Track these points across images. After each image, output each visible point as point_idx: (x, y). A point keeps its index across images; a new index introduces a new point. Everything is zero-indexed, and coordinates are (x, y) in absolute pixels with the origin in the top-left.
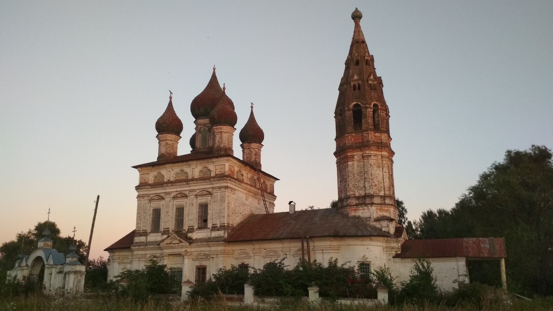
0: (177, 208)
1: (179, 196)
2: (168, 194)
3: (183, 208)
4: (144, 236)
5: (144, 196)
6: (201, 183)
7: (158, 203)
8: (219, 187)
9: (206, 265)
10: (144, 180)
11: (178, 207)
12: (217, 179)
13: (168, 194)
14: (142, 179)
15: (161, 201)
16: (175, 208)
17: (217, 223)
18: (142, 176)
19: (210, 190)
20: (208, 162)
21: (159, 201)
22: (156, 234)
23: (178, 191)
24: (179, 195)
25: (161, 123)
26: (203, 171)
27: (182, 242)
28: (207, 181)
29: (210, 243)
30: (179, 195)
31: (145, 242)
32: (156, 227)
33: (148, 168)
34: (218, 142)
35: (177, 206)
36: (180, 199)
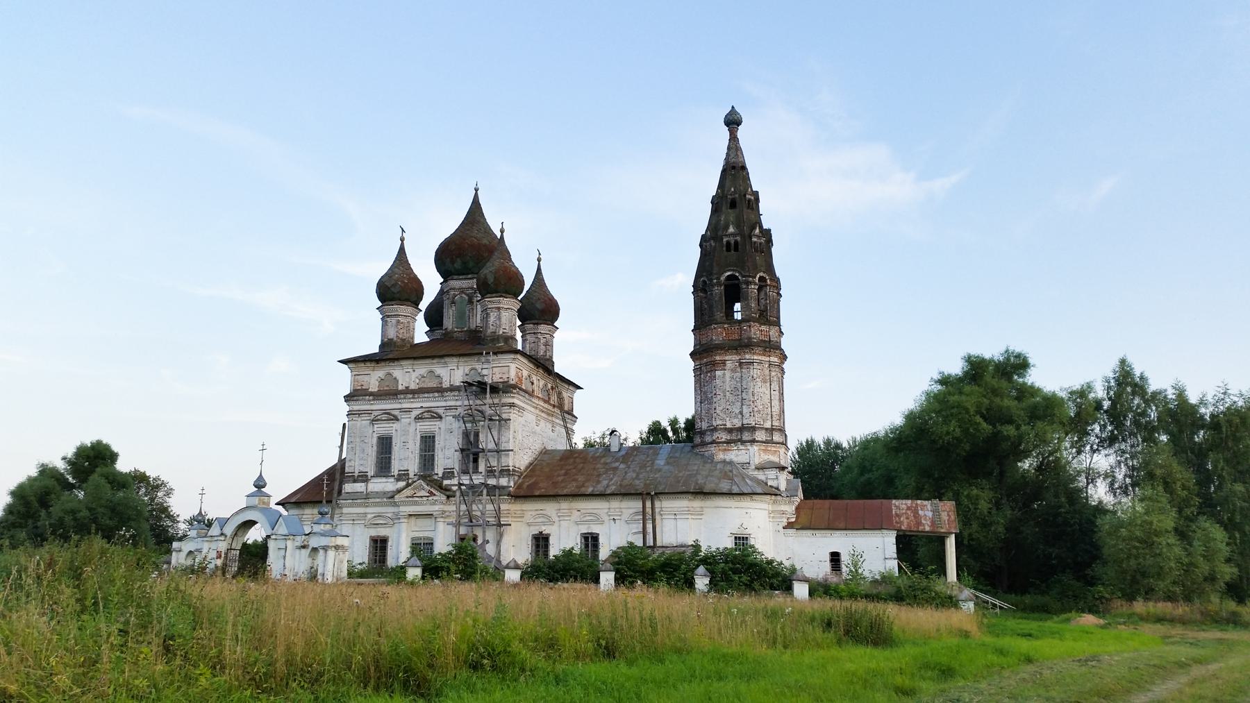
2: (405, 412)
3: (434, 437)
4: (363, 481)
5: (361, 414)
7: (387, 425)
10: (360, 384)
13: (405, 412)
14: (356, 383)
15: (393, 423)
16: (419, 437)
21: (389, 423)
22: (384, 480)
25: (389, 286)
30: (426, 415)
32: (384, 467)
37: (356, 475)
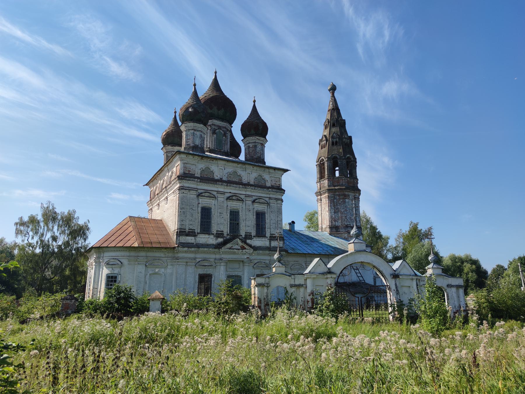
3: (238, 212)
8: (276, 198)
15: (213, 200)
21: (210, 199)
22: (207, 236)
27: (245, 249)
32: (206, 227)
37: (187, 230)
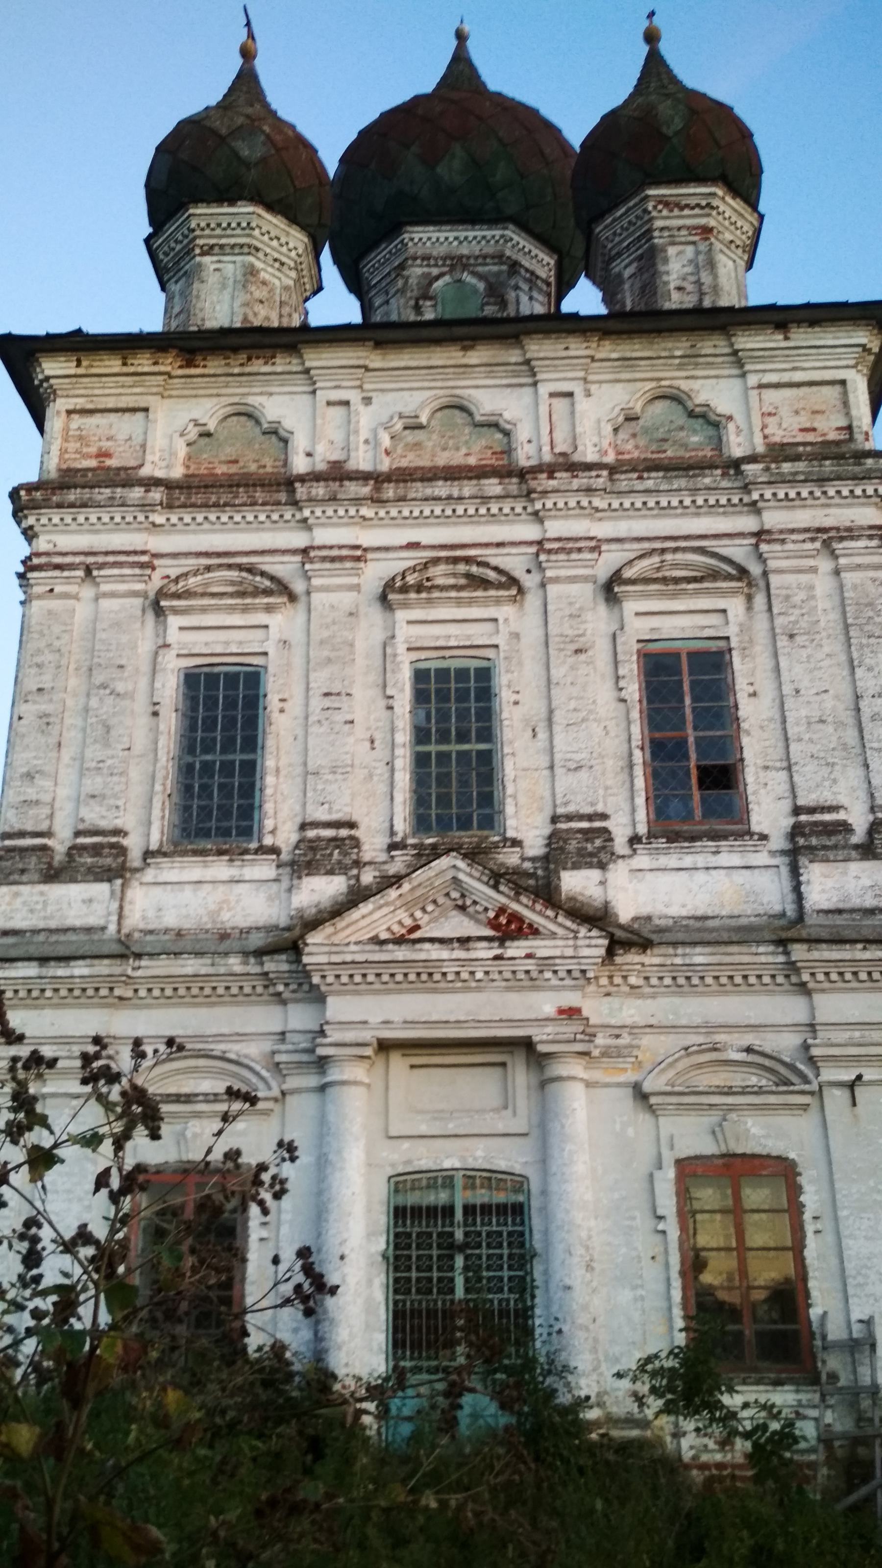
0: (420, 676)
1: (440, 581)
2: (333, 559)
3: (485, 675)
4: (106, 875)
5: (102, 566)
6: (647, 491)
7: (237, 619)
8: (819, 530)
9: (792, 1155)
10: (93, 450)
11: (433, 665)
12: (801, 466)
13: (333, 559)
14: (73, 446)
15: (269, 609)
16: (406, 675)
17: (843, 800)
18: (74, 425)
19: (738, 551)
20: (692, 358)
21: (245, 609)
23: (426, 547)
24: (442, 568)
25: (224, 131)
26: (641, 422)
27: (534, 932)
28: (707, 481)
29: (816, 955)
30: (440, 574)
31: (112, 928)
33: (143, 362)
34: (680, 289)
35: (423, 655)
36: (459, 602)
37: (60, 844)
